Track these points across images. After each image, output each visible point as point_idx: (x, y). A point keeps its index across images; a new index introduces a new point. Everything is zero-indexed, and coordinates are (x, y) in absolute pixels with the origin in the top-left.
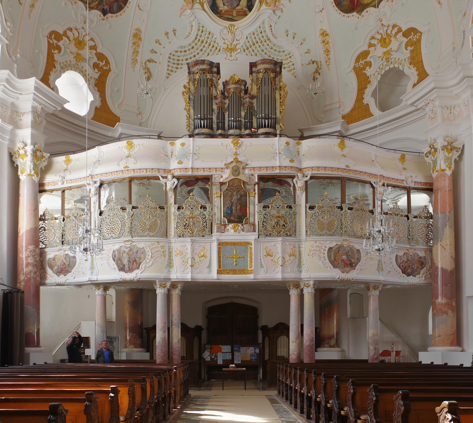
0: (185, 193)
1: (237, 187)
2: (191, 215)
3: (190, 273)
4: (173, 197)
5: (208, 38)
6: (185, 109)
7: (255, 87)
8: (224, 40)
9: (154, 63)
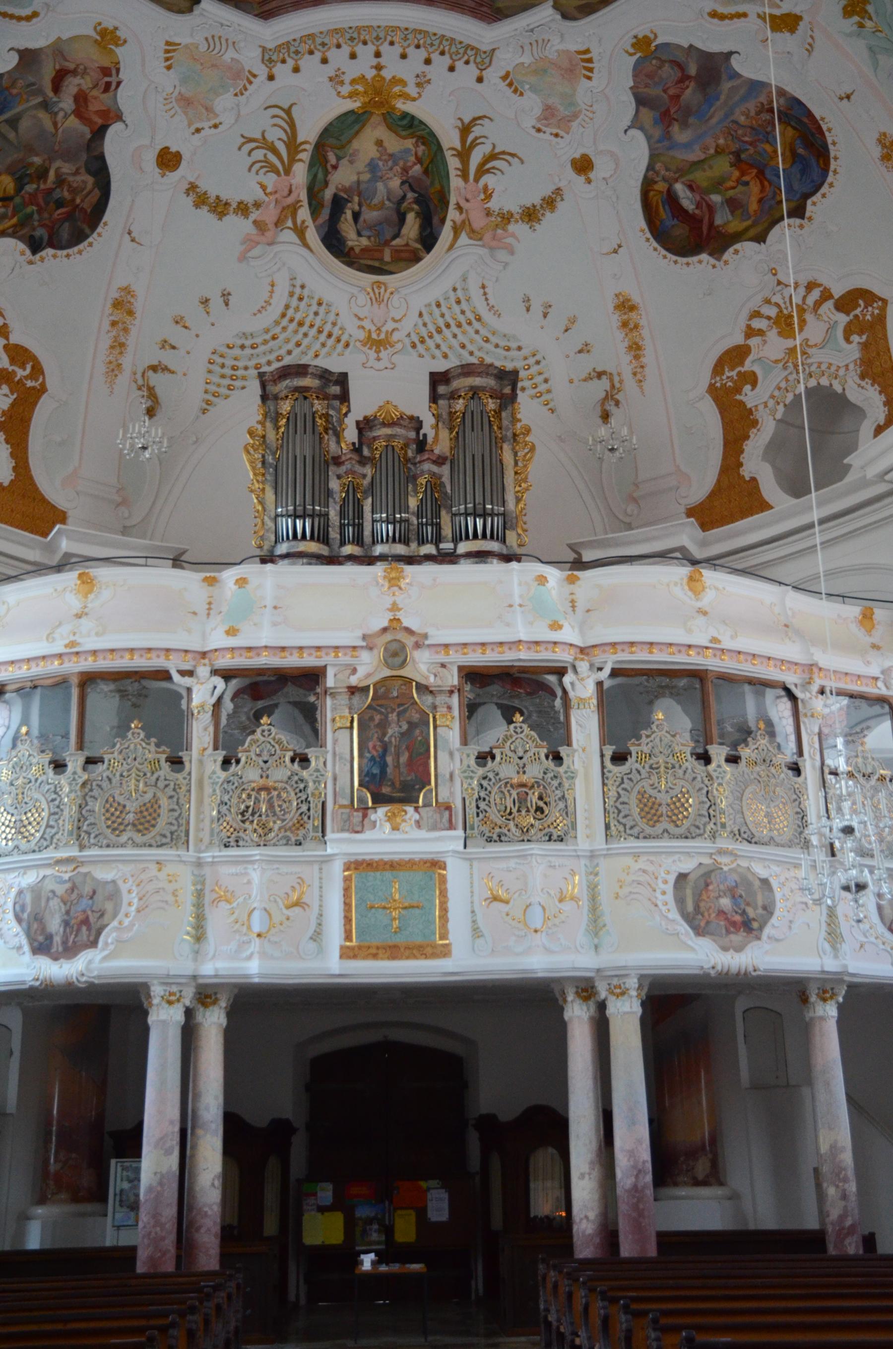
0: (248, 718)
1: (398, 701)
2: (262, 782)
3: (256, 956)
4: (211, 729)
5: (316, 314)
6: (252, 491)
7: (444, 434)
8: (360, 319)
9: (168, 375)
